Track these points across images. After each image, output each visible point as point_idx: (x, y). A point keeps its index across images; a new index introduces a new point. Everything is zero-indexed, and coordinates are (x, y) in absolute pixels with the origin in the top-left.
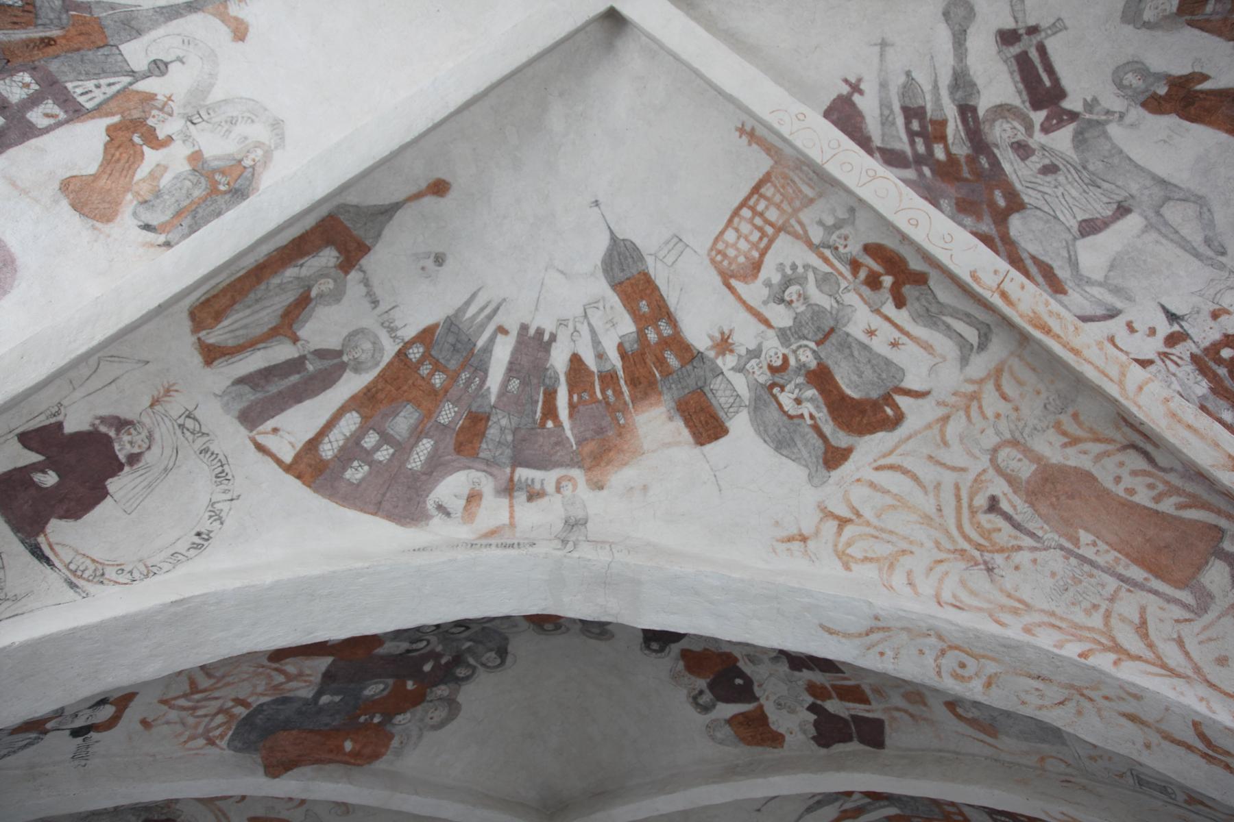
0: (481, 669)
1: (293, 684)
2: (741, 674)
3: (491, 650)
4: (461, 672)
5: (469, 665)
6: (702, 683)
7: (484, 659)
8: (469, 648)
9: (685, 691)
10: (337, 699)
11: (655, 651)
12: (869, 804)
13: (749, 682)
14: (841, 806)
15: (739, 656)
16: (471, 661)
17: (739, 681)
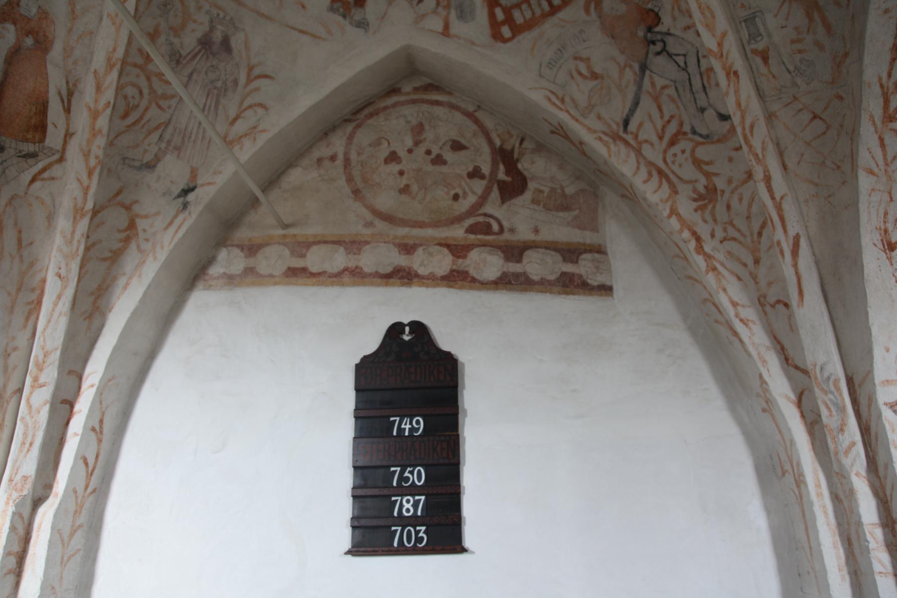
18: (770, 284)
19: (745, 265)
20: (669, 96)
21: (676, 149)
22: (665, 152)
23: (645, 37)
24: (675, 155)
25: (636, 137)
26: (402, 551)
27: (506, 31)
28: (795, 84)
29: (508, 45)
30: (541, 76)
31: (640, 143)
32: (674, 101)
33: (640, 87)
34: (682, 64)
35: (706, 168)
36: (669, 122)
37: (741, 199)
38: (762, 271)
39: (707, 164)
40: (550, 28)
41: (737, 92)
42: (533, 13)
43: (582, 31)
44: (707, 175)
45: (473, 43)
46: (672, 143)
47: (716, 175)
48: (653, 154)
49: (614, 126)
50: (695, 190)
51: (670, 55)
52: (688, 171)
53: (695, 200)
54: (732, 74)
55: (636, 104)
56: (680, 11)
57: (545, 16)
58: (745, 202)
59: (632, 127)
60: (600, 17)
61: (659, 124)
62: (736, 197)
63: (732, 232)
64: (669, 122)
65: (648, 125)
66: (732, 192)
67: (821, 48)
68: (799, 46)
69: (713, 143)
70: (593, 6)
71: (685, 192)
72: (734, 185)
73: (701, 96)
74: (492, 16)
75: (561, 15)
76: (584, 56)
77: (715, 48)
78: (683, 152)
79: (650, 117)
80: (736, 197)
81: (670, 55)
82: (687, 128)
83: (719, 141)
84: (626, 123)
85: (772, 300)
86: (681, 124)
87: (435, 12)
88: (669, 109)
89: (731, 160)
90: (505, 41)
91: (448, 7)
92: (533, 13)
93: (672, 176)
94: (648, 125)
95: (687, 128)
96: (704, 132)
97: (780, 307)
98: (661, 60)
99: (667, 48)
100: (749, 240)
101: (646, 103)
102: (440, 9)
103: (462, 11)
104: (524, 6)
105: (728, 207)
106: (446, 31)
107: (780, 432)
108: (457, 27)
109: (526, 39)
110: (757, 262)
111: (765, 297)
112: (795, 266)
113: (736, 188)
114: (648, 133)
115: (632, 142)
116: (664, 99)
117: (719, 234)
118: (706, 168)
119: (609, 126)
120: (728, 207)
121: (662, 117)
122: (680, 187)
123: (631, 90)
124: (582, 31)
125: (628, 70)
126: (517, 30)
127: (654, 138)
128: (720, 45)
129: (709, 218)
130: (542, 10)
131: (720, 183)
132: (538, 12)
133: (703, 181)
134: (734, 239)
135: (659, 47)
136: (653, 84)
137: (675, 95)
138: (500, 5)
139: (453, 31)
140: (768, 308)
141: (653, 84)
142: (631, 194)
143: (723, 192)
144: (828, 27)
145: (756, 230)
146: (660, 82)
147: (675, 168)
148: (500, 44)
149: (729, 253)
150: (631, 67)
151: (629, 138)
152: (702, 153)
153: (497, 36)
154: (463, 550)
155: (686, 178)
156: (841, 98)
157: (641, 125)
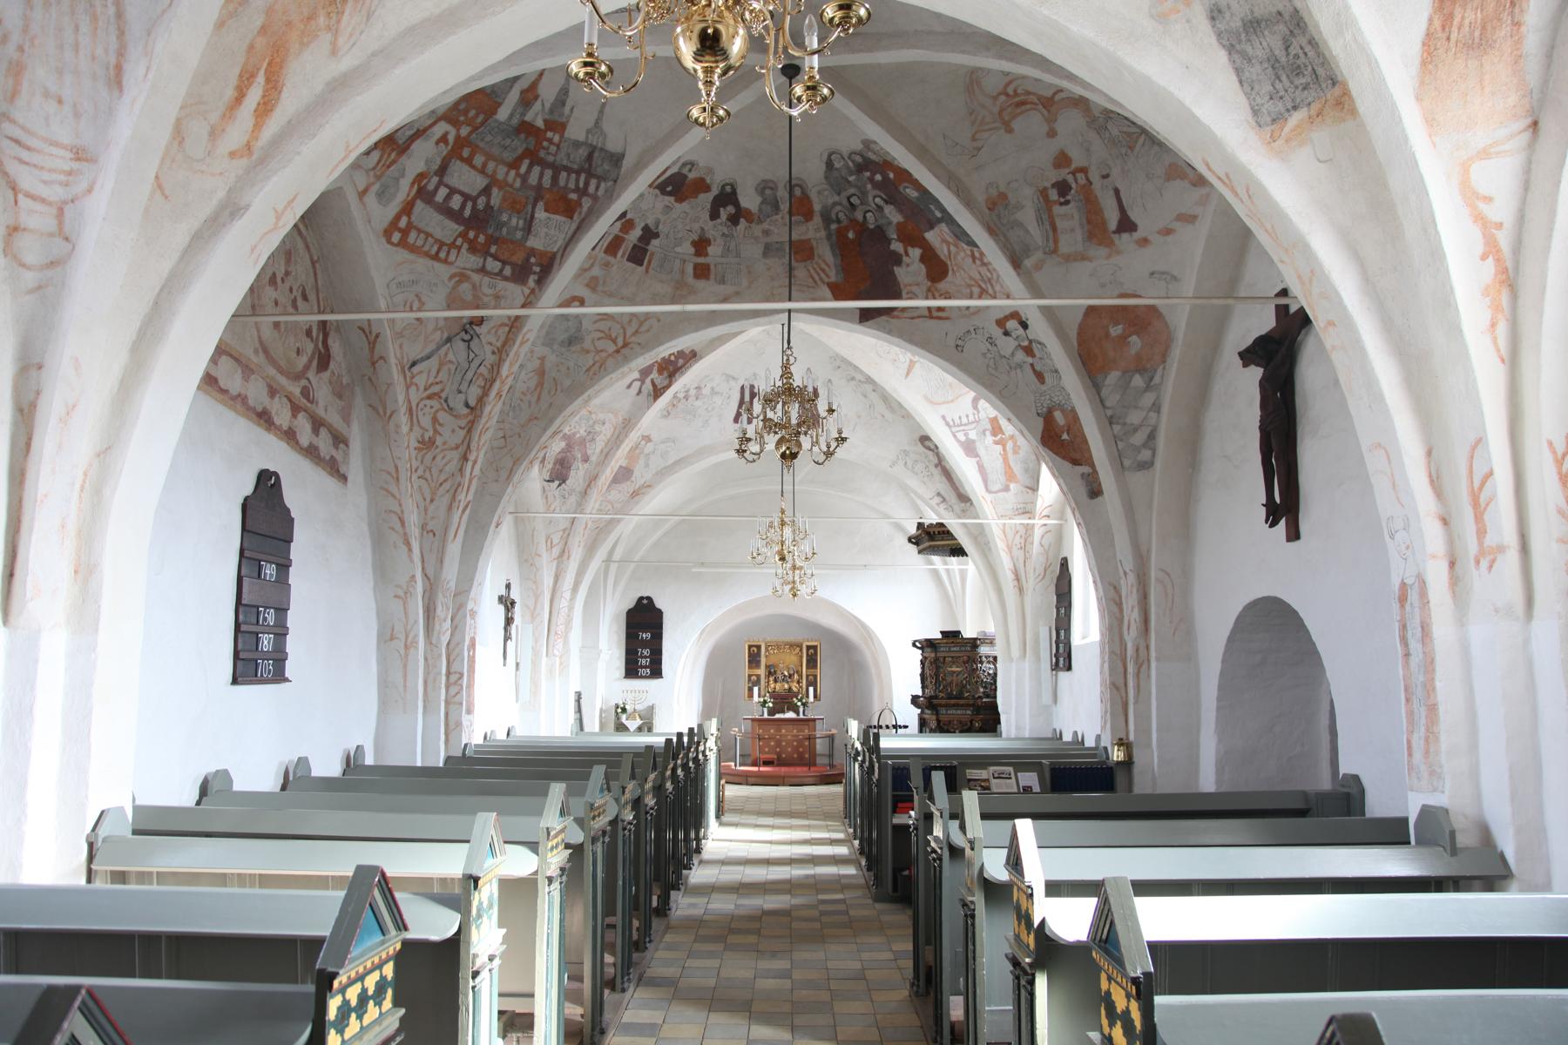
0: (846, 156)
1: (951, 240)
2: (670, 194)
3: (837, 169)
4: (858, 159)
5: (853, 161)
6: (692, 176)
7: (842, 163)
8: (851, 175)
9: (701, 165)
10: (932, 206)
11: (728, 184)
12: (523, 114)
13: (664, 192)
14: (543, 105)
15: (676, 204)
16: (850, 164)
17: (669, 189)
18: (433, 518)
19: (425, 500)
20: (449, 370)
21: (428, 402)
22: (422, 400)
23: (465, 325)
24: (425, 406)
25: (413, 377)
26: (642, 677)
27: (396, 237)
28: (508, 414)
29: (389, 246)
30: (388, 285)
31: (412, 383)
32: (450, 374)
33: (438, 349)
34: (471, 358)
35: (437, 426)
36: (437, 383)
37: (443, 458)
38: (432, 508)
39: (441, 425)
40: (422, 263)
41: (495, 405)
42: (423, 246)
43: (436, 285)
44: (435, 431)
45: (369, 222)
46: (429, 397)
47: (440, 434)
48: (414, 396)
49: (405, 360)
50: (422, 436)
51: (469, 347)
52: (426, 421)
53: (419, 442)
54: (499, 395)
55: (428, 357)
56: (496, 332)
57: (427, 255)
58: (444, 461)
59: (416, 369)
60: (454, 288)
61: (431, 380)
62: (442, 455)
63: (427, 475)
64: (437, 383)
65: (424, 376)
66: (442, 451)
67: (530, 406)
68: (522, 397)
69: (451, 415)
70: (457, 279)
71: (417, 432)
72: (445, 447)
73: (465, 384)
74: (398, 217)
75: (436, 264)
76: (423, 299)
77: (504, 377)
78: (432, 407)
79: (430, 371)
80: (442, 455)
81: (469, 347)
82: (443, 395)
83: (455, 416)
84: (414, 364)
85: (429, 528)
86: (442, 391)
87: (367, 171)
88: (443, 376)
89: (453, 431)
90: (389, 242)
91: (378, 178)
92: (423, 246)
93: (415, 417)
94: (424, 376)
95: (443, 395)
96: (451, 405)
97: (431, 534)
98: (462, 346)
99: (471, 343)
100: (434, 484)
101: (434, 362)
102: (372, 173)
103: (383, 192)
104: (422, 235)
105: (434, 458)
106: (363, 194)
107: (406, 613)
108: (371, 198)
109: (404, 254)
110: (432, 501)
111: (426, 524)
112: (461, 518)
113: (445, 450)
114: (421, 380)
115: (408, 379)
116: (445, 368)
117: (420, 472)
118: (437, 426)
119: (403, 358)
120: (434, 458)
121: (436, 377)
122: (416, 428)
123: (432, 346)
124: (436, 285)
125: (439, 332)
126: (403, 244)
127: (422, 388)
128: (507, 377)
129: (420, 458)
130: (430, 250)
131: (439, 441)
132: (426, 248)
133: (431, 433)
134: (426, 480)
135: (467, 337)
136: (446, 354)
137: (453, 372)
138: (409, 218)
139: (367, 199)
140: (425, 533)
141: (446, 354)
142: (385, 413)
143: (437, 447)
144: (539, 399)
145: (441, 481)
146: (451, 356)
147: (420, 413)
148: (383, 240)
149: (420, 487)
150: (443, 332)
151: (408, 374)
152: (442, 416)
153: (387, 233)
154: (287, 680)
155: (423, 424)
156: (520, 436)
157: (421, 372)
